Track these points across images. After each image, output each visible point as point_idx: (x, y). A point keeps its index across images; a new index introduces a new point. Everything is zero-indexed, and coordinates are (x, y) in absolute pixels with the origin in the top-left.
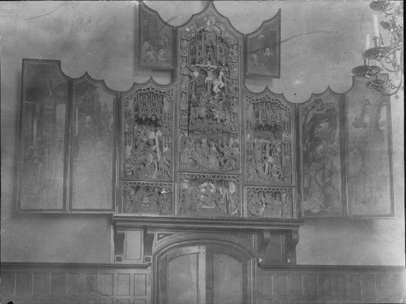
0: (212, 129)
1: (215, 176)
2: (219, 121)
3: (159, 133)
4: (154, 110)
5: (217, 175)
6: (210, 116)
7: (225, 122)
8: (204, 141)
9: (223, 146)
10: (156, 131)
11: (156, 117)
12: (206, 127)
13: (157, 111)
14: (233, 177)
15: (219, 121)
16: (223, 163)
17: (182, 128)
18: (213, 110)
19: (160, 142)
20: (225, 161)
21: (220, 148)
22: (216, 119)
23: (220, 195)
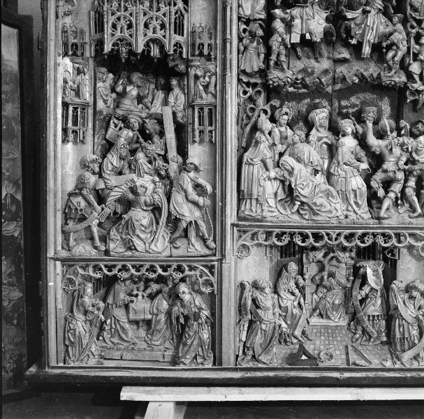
0: (344, 79)
1: (352, 235)
2: (367, 50)
3: (178, 98)
4: (155, 23)
5: (360, 232)
6: (339, 33)
7: (390, 54)
8: (321, 116)
9: (380, 135)
10: (168, 89)
11: (162, 47)
12: (326, 72)
13: (163, 26)
14: (411, 235)
15: (367, 50)
16: (381, 193)
17: (245, 79)
18: (349, 15)
19: (180, 129)
20: (387, 184)
21: (372, 140)
22: (360, 45)
23: (366, 289)
